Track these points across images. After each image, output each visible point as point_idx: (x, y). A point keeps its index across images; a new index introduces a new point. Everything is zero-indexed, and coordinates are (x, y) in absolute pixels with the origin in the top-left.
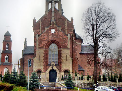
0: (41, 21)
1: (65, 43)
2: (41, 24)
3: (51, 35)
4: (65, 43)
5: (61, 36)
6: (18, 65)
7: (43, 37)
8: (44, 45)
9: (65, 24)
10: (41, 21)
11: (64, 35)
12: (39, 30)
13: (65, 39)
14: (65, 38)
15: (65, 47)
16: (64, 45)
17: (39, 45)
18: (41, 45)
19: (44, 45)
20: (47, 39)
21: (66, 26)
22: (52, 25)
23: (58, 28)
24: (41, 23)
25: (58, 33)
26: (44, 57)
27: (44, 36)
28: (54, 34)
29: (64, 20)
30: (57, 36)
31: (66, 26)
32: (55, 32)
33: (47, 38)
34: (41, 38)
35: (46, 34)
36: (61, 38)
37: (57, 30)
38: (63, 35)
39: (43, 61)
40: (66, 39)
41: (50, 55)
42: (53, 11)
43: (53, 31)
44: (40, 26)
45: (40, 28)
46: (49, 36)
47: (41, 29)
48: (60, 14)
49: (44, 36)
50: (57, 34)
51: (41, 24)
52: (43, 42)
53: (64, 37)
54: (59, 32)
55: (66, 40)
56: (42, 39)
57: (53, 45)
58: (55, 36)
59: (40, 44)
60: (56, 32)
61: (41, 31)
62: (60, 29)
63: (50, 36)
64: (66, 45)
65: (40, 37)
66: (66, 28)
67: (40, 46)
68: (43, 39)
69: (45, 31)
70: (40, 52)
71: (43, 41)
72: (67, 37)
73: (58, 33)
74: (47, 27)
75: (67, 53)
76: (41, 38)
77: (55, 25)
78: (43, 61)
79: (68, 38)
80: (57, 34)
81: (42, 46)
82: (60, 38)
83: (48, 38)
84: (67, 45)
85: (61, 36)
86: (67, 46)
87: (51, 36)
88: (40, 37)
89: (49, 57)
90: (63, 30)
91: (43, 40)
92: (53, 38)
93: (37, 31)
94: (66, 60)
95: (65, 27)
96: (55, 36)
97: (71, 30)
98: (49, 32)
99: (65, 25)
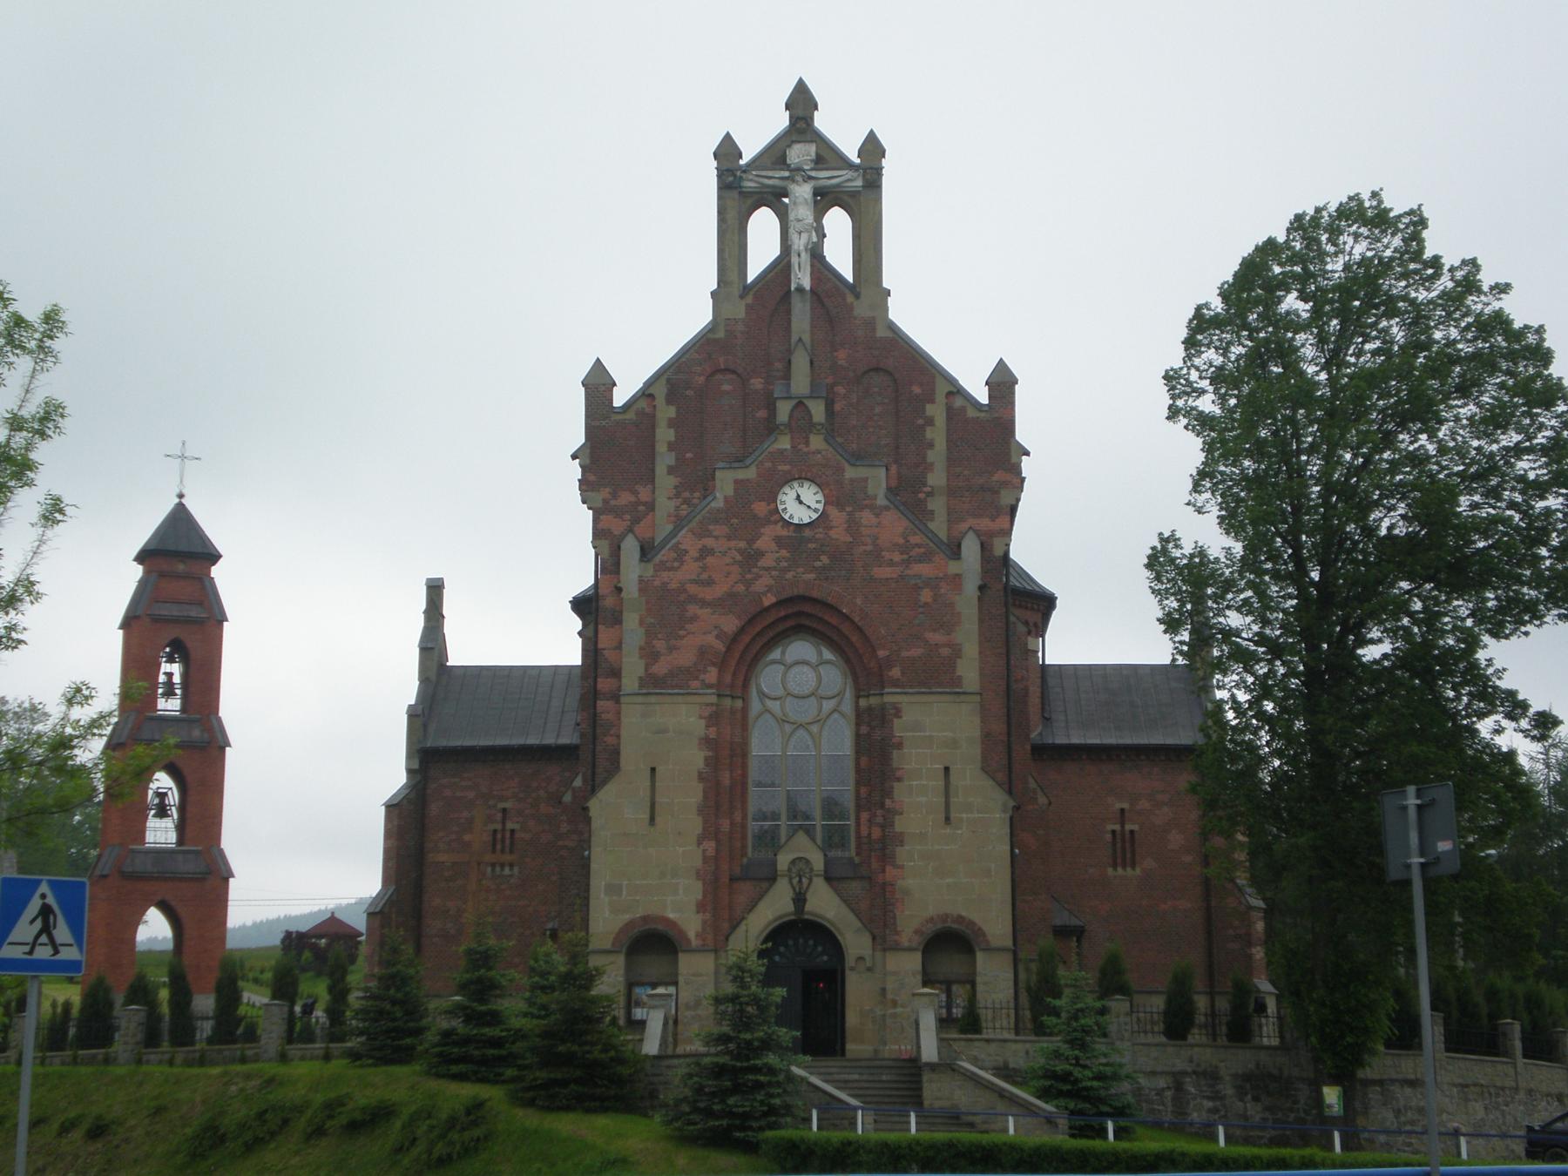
0: (670, 400)
1: (930, 636)
2: (671, 423)
3: (779, 541)
4: (930, 636)
5: (891, 563)
7: (690, 569)
8: (702, 652)
9: (922, 428)
12: (644, 494)
13: (926, 596)
15: (935, 675)
16: (916, 652)
17: (650, 655)
18: (671, 649)
19: (702, 652)
20: (741, 588)
21: (937, 455)
22: (784, 443)
23: (850, 473)
24: (671, 412)
26: (710, 778)
29: (917, 390)
31: (937, 455)
32: (824, 515)
35: (726, 529)
39: (699, 830)
42: (800, 290)
43: (801, 504)
44: (661, 448)
45: (661, 469)
46: (761, 554)
47: (665, 482)
49: (705, 552)
51: (671, 423)
52: (694, 618)
53: (918, 568)
54: (866, 517)
57: (801, 649)
58: (825, 560)
59: (660, 645)
60: (834, 512)
61: (665, 505)
62: (877, 480)
64: (945, 651)
65: (662, 566)
66: (937, 478)
67: (660, 668)
68: (693, 589)
71: (693, 609)
72: (953, 567)
73: (853, 526)
74: (739, 460)
76: (674, 579)
77: (817, 442)
78: (695, 825)
79: (958, 576)
80: (839, 534)
83: (748, 584)
84: (957, 652)
85: (891, 563)
87: (784, 553)
88: (662, 566)
90: (908, 494)
92: (804, 579)
93: (625, 498)
94: (948, 819)
95: (924, 467)
96: (825, 560)
98: (760, 508)
99: (931, 445)
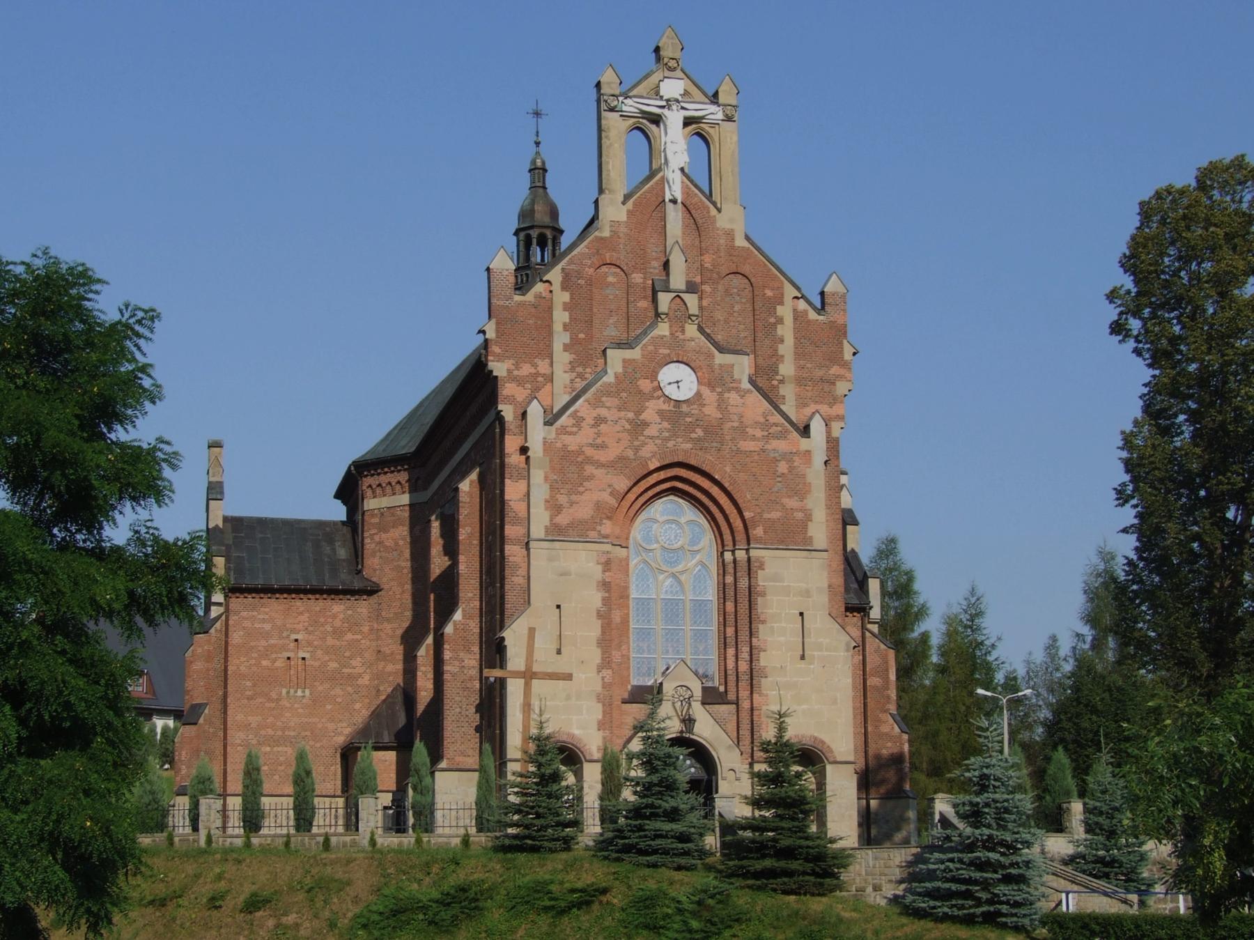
0: (565, 287)
1: (785, 501)
2: (566, 307)
3: (661, 413)
4: (785, 501)
5: (754, 438)
6: (536, 668)
7: (586, 435)
8: (598, 506)
9: (775, 325)
10: (565, 287)
11: (773, 430)
12: (543, 366)
13: (783, 467)
14: (788, 457)
15: (792, 536)
16: (775, 515)
17: (555, 508)
18: (572, 504)
19: (598, 506)
20: (630, 453)
21: (787, 348)
22: (663, 329)
23: (720, 359)
24: (566, 297)
25: (722, 405)
26: (604, 616)
27: (599, 421)
28: (684, 408)
29: (769, 293)
30: (713, 431)
31: (787, 348)
32: (698, 395)
33: (625, 443)
34: (568, 439)
35: (616, 402)
36: (749, 453)
37: (714, 380)
38: (766, 425)
39: (598, 660)
40: (797, 462)
41: (644, 603)
42: (674, 201)
43: (679, 381)
44: (558, 327)
45: (558, 346)
46: (645, 424)
47: (562, 358)
48: (730, 235)
49: (599, 421)
50: (711, 411)
51: (566, 307)
52: (590, 478)
53: (775, 444)
54: (733, 397)
55: (791, 469)
56: (580, 452)
57: (665, 508)
58: (700, 432)
59: (563, 499)
60: (706, 392)
61: (562, 377)
62: (743, 366)
63: (652, 431)
64: (799, 515)
65: (563, 431)
66: (787, 368)
67: (563, 519)
68: (589, 451)
69: (609, 378)
70: (565, 574)
71: (590, 469)
72: (804, 444)
73: (722, 405)
74: (624, 345)
75: (807, 594)
76: (572, 442)
77: (691, 330)
78: (595, 656)
79: (808, 452)
80: (711, 411)
81: (584, 510)
82: (739, 451)
83: (637, 449)
84: (808, 517)
85: (754, 438)
86: (805, 527)
87: (666, 425)
88: (563, 431)
89: (633, 625)
90: (764, 382)
91: (589, 460)
92: (683, 448)
93: (526, 369)
94: (803, 657)
95: (777, 358)
96: (700, 432)
97: (827, 387)
98: (645, 385)
99: (782, 341)
